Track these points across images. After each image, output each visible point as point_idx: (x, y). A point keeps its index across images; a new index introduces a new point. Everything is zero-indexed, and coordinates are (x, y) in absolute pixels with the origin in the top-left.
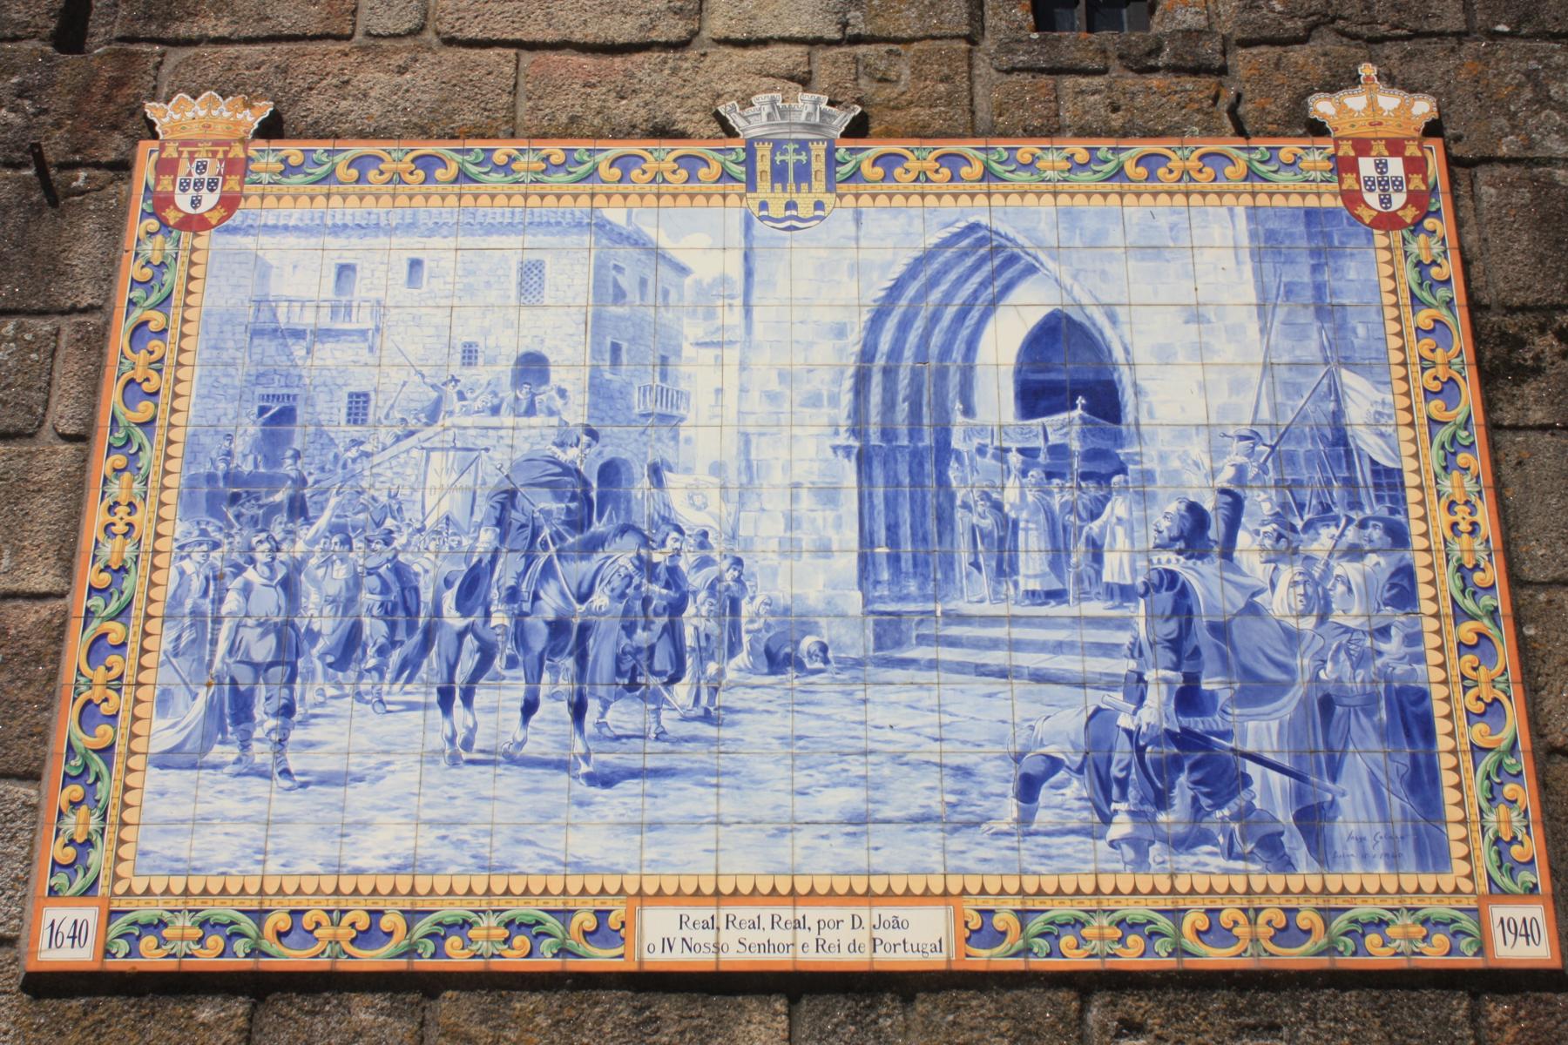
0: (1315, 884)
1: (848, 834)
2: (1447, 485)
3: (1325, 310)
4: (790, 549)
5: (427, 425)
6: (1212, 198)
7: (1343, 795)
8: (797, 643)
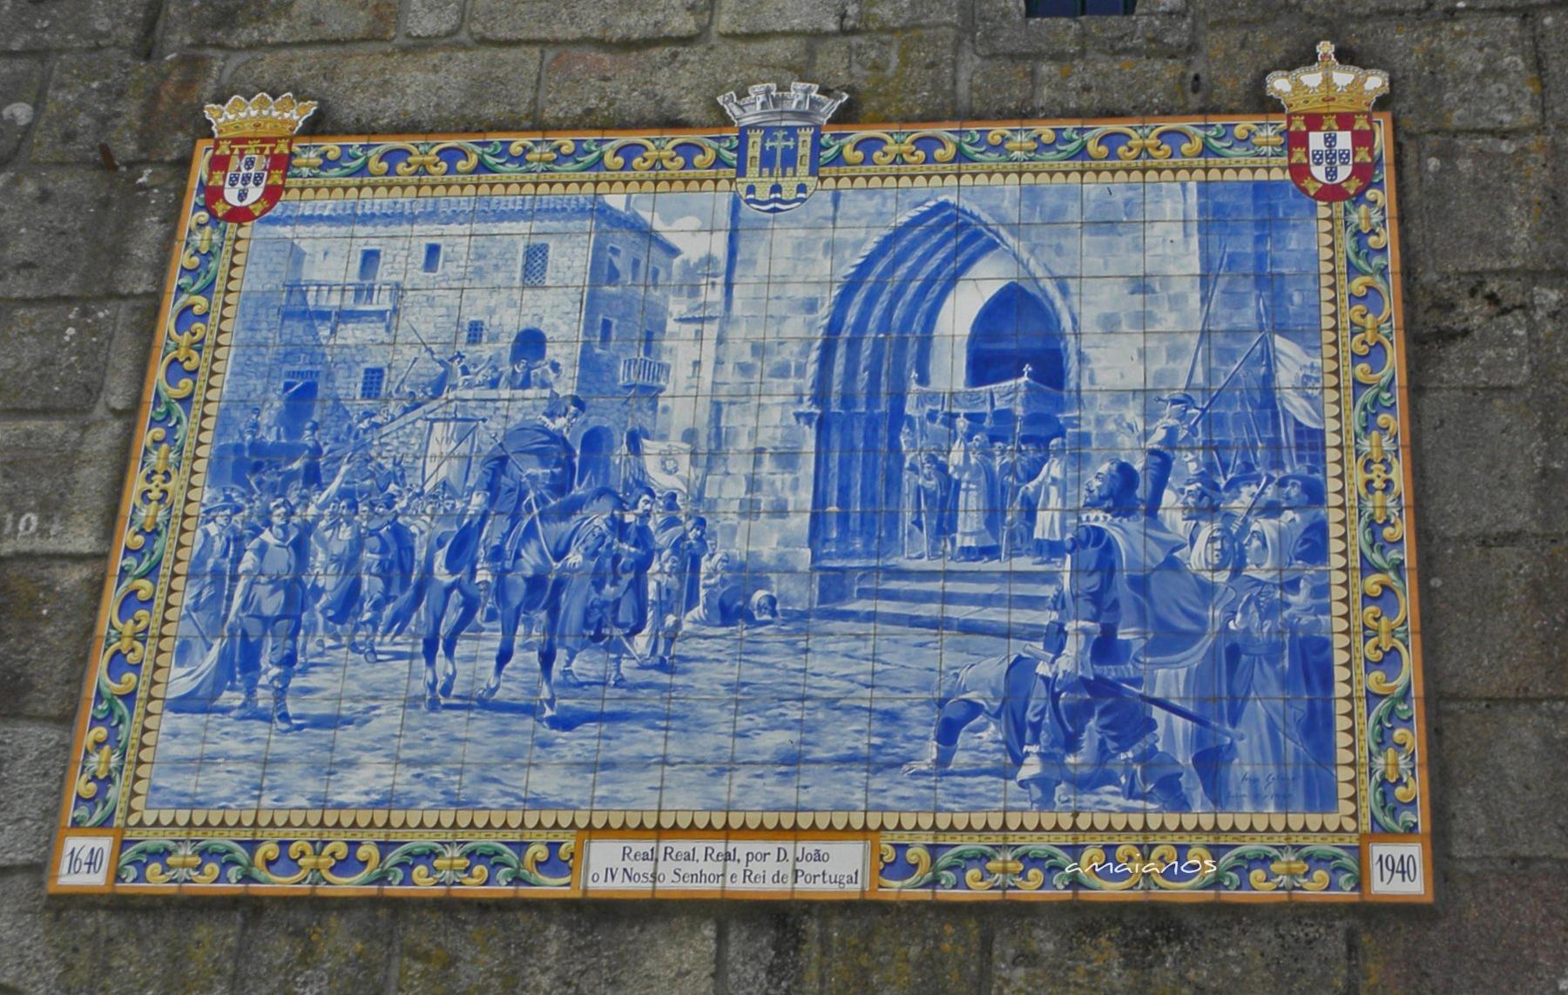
0: (1207, 822)
1: (781, 773)
2: (1366, 445)
3: (1268, 281)
5: (433, 398)
6: (1167, 174)
7: (1242, 738)
8: (749, 597)
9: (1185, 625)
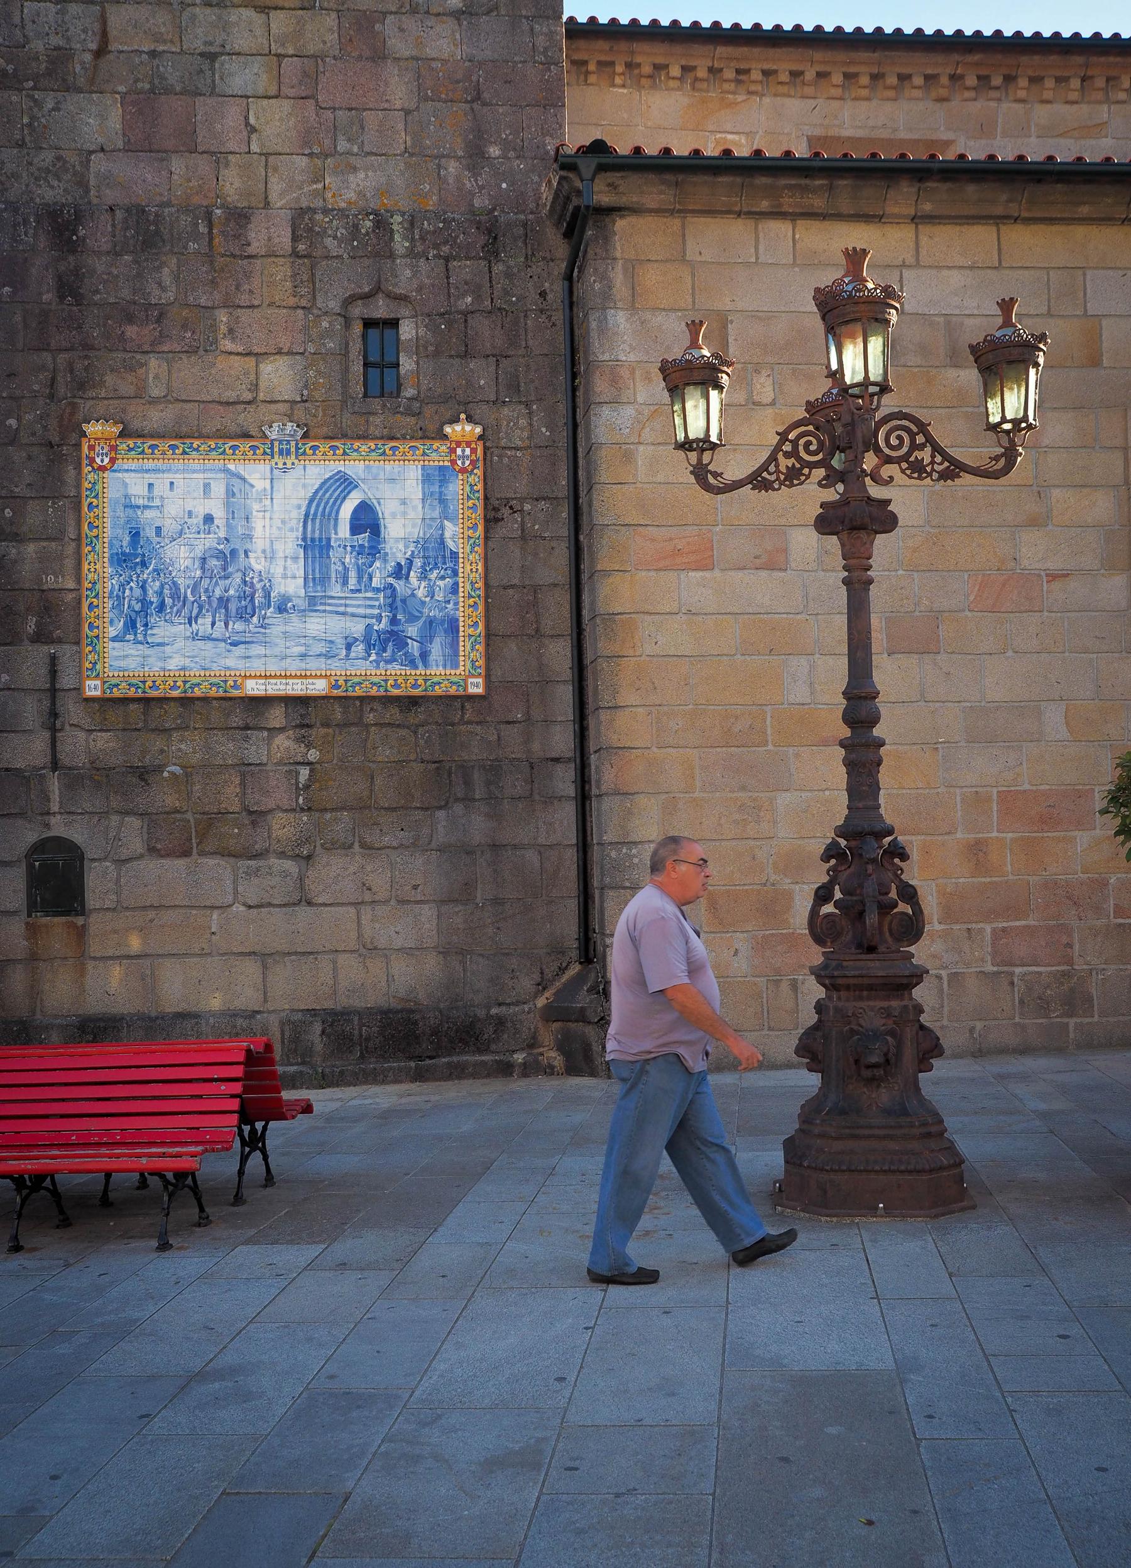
3: (442, 501)
4: (285, 577)
9: (417, 614)
